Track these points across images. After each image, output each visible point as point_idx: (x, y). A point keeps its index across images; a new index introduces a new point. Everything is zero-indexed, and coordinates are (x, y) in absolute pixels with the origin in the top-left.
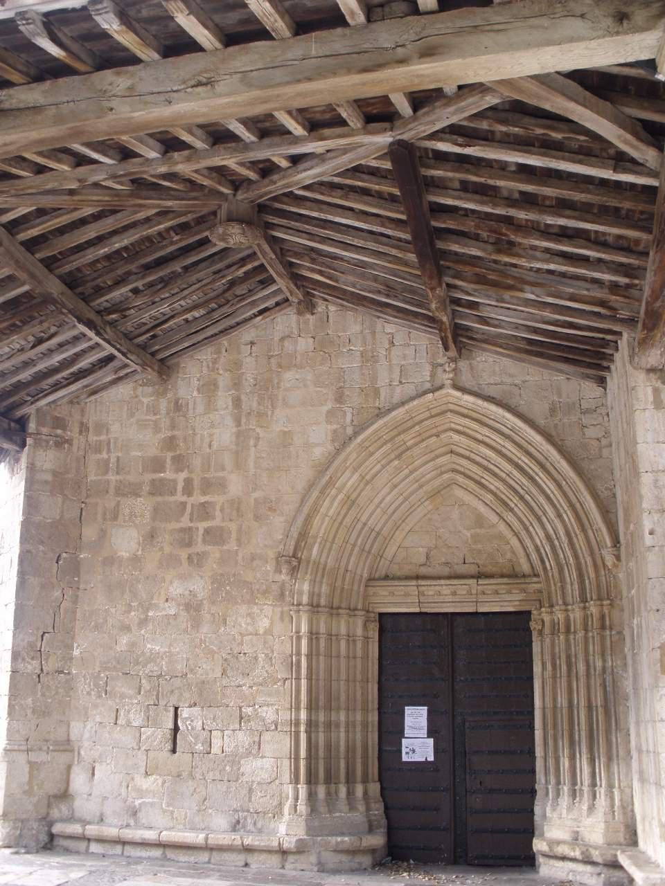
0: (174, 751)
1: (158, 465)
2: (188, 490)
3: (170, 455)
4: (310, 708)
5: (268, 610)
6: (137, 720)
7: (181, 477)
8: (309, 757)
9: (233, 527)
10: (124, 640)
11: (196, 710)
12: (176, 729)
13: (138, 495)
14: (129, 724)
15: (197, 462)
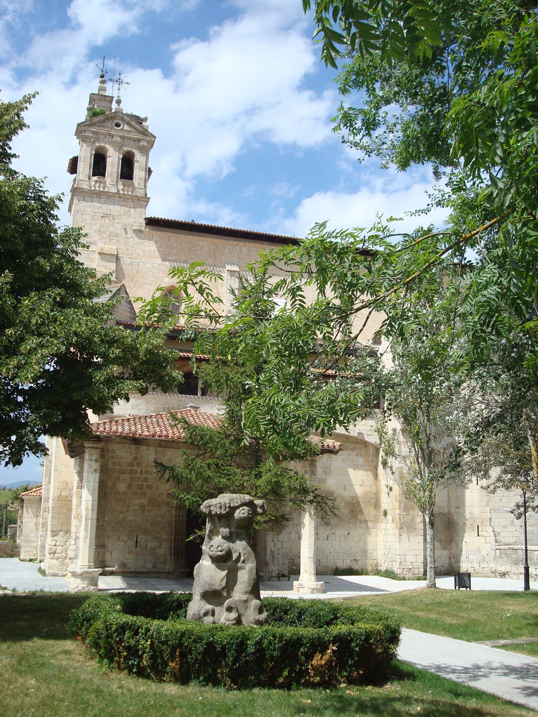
0: (136, 547)
1: (131, 465)
2: (141, 473)
3: (135, 462)
4: (175, 536)
5: (164, 508)
6: (125, 539)
7: (139, 469)
8: (174, 549)
9: (155, 485)
10: (122, 516)
11: (143, 536)
12: (137, 541)
13: (125, 473)
14: (123, 540)
15: (144, 465)
